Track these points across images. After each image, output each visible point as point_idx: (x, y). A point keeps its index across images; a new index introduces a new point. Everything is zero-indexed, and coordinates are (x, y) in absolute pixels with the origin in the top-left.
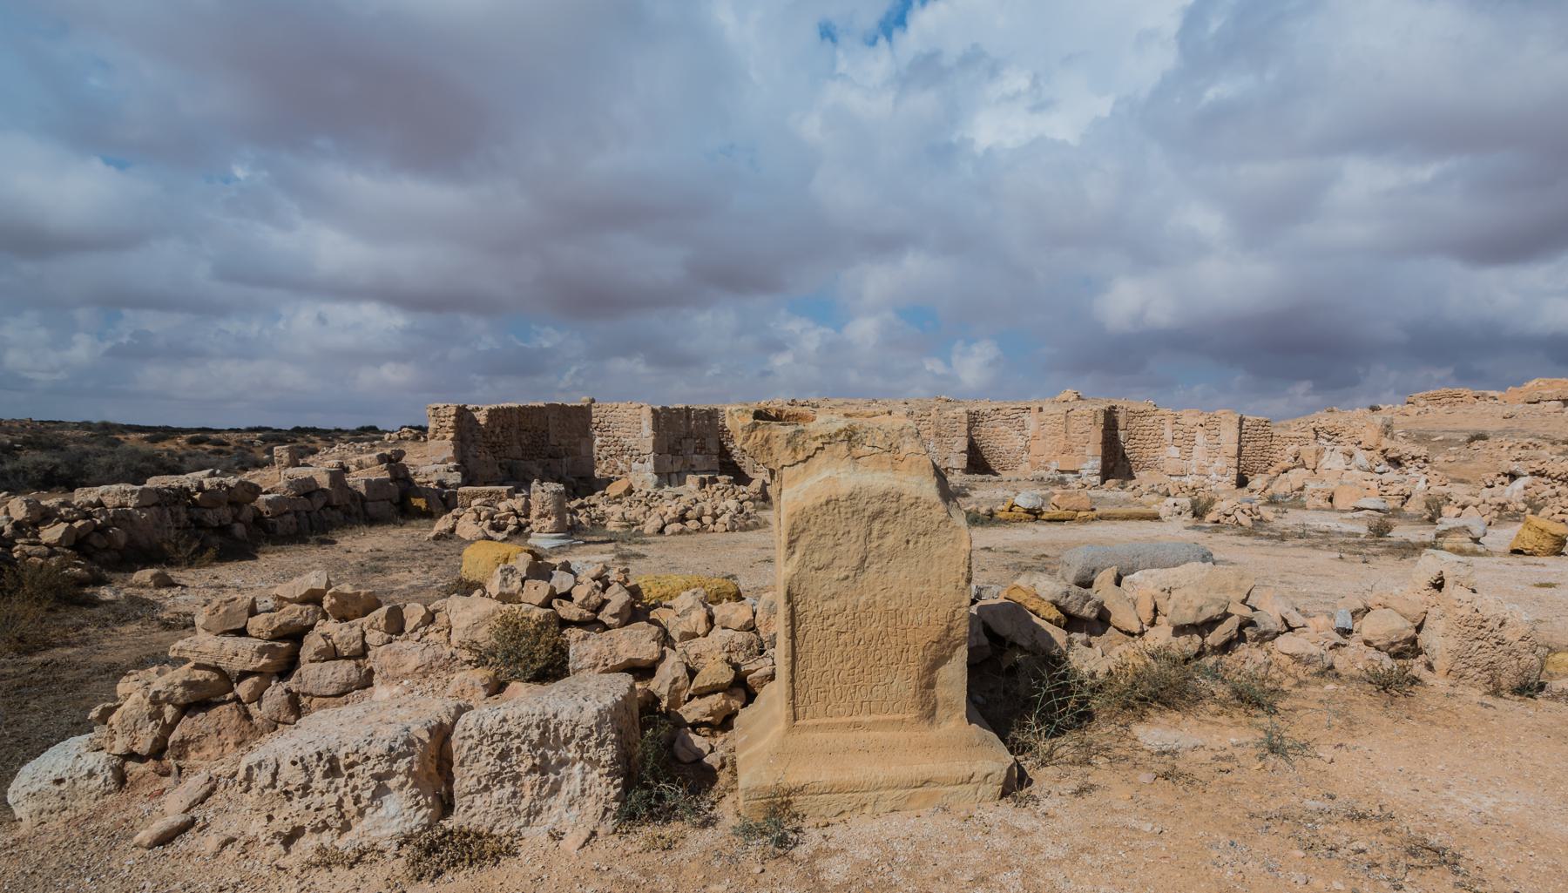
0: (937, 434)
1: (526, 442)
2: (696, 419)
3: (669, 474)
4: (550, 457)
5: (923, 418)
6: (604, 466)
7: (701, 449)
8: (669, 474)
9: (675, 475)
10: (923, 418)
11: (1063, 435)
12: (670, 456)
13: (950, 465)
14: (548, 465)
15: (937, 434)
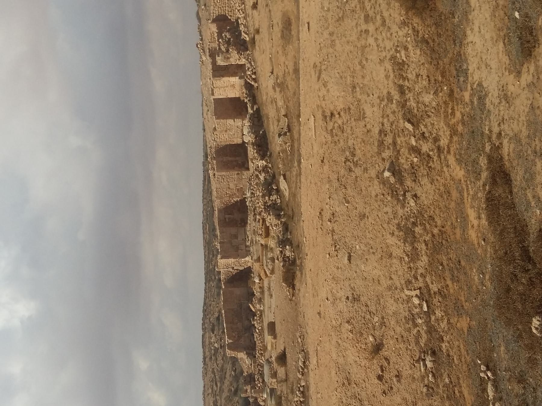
0: (226, 131)
1: (237, 320)
2: (223, 239)
3: (246, 251)
4: (241, 309)
5: (218, 137)
6: (243, 265)
7: (236, 237)
8: (246, 251)
9: (247, 248)
10: (218, 137)
11: (226, 88)
12: (239, 251)
13: (241, 126)
14: (244, 309)
15: (226, 131)
